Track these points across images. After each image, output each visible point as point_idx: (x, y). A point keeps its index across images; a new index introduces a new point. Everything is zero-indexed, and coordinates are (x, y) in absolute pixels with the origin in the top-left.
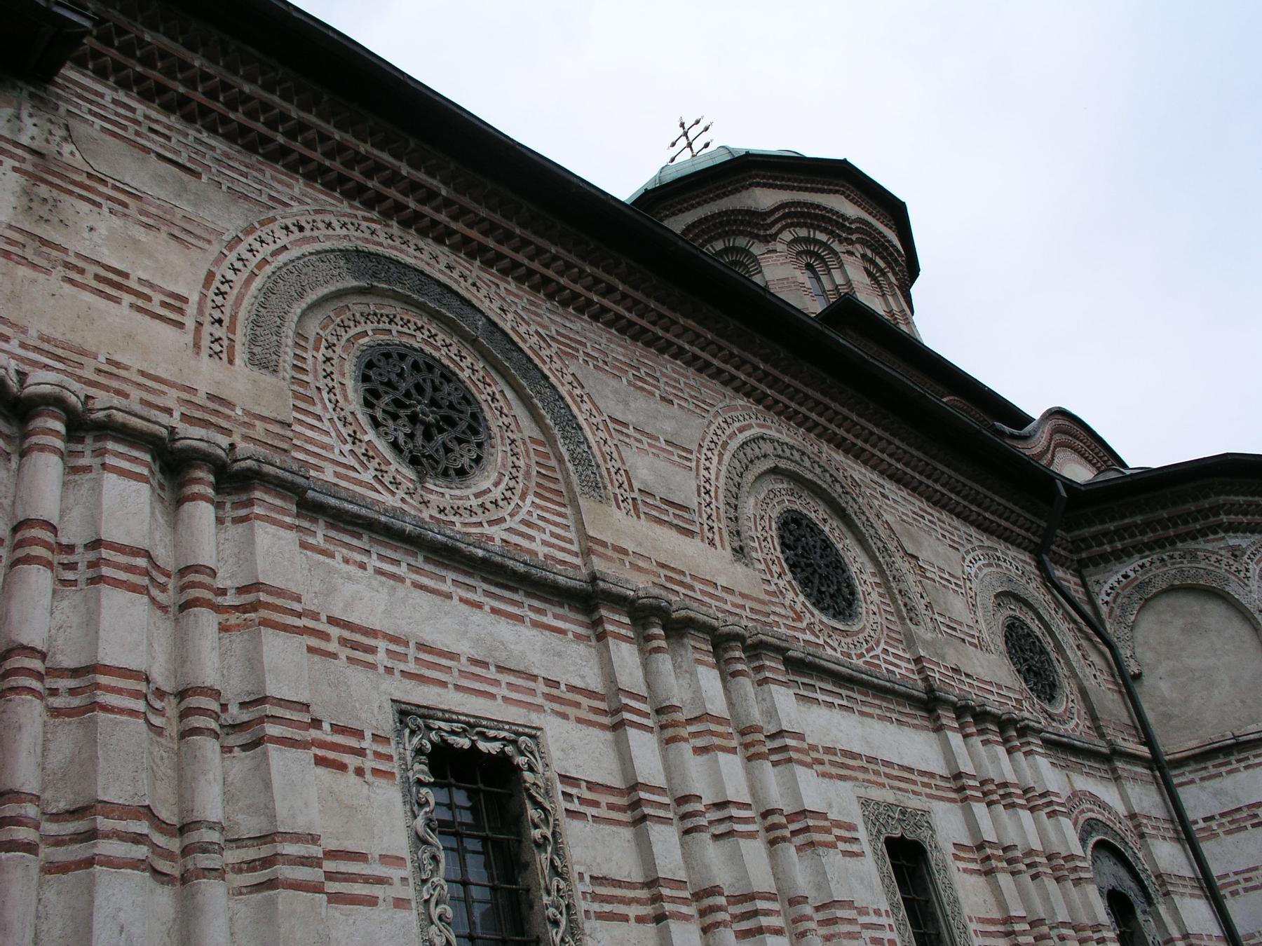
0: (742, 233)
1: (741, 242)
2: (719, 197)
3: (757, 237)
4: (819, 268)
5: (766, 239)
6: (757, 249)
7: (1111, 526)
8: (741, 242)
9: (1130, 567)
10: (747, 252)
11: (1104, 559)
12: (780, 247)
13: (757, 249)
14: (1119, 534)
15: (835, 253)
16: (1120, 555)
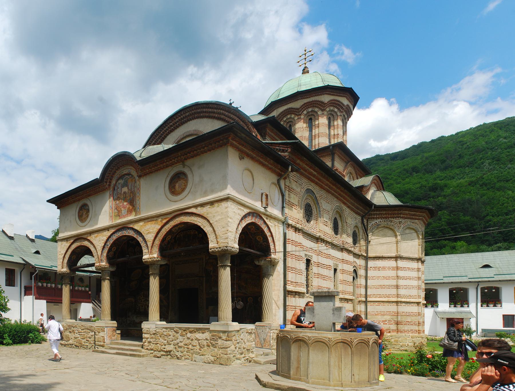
0: (318, 107)
1: (316, 109)
2: (316, 96)
3: (321, 109)
4: (332, 119)
5: (323, 110)
6: (320, 113)
7: (378, 213)
8: (316, 109)
9: (378, 221)
10: (317, 113)
11: (374, 218)
12: (325, 113)
13: (320, 113)
14: (379, 214)
15: (337, 115)
16: (376, 218)
